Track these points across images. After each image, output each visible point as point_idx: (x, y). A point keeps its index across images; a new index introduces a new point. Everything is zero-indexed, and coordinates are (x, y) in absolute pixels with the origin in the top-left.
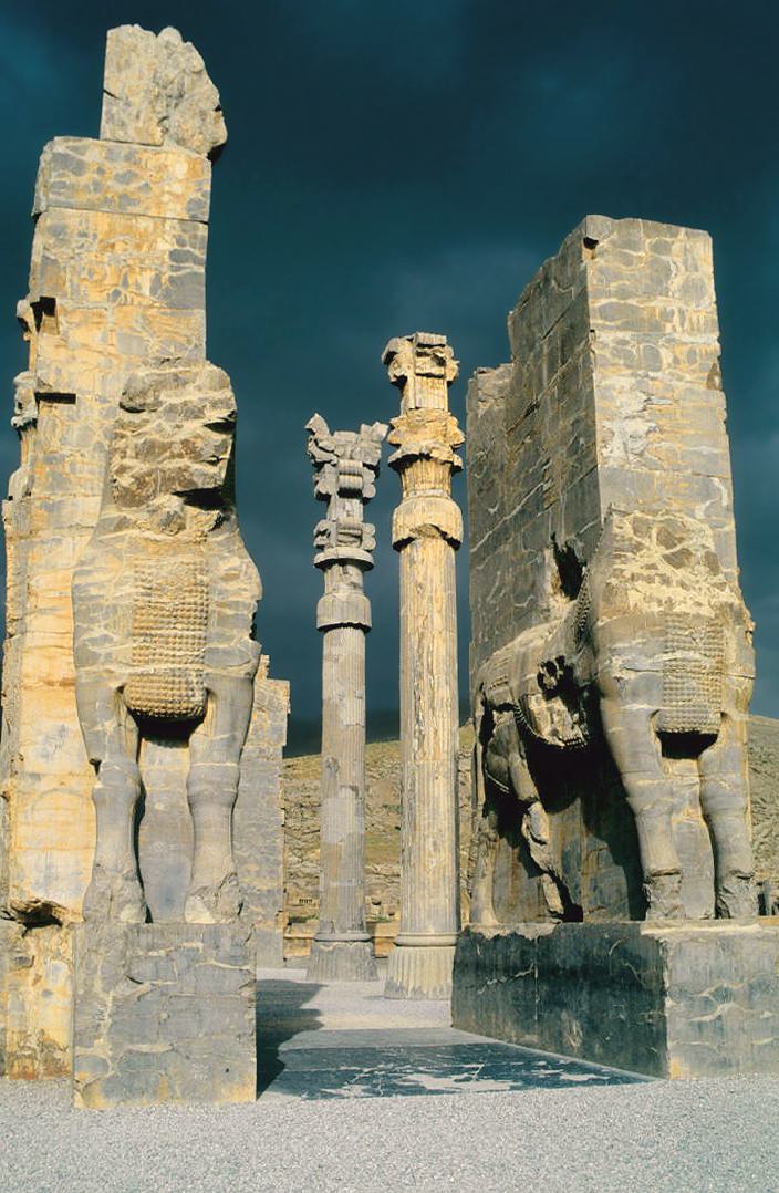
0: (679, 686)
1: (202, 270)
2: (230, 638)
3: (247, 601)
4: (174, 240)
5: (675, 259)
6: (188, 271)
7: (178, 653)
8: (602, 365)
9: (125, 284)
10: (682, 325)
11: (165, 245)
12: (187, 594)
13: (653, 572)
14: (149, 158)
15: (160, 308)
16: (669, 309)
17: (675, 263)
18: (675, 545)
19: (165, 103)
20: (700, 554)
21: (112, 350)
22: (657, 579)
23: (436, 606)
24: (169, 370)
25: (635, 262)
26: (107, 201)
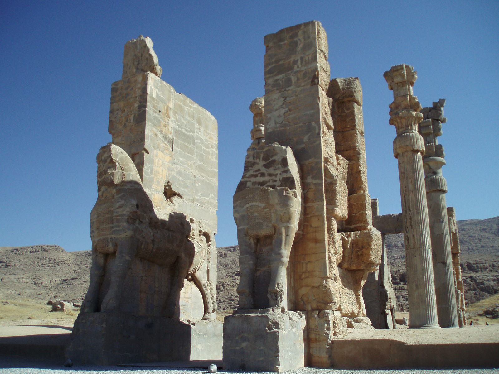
4: (139, 102)
6: (142, 110)
9: (127, 121)
10: (301, 64)
11: (136, 105)
13: (257, 173)
16: (296, 59)
17: (299, 39)
18: (269, 159)
20: (280, 160)
21: (123, 142)
22: (259, 175)
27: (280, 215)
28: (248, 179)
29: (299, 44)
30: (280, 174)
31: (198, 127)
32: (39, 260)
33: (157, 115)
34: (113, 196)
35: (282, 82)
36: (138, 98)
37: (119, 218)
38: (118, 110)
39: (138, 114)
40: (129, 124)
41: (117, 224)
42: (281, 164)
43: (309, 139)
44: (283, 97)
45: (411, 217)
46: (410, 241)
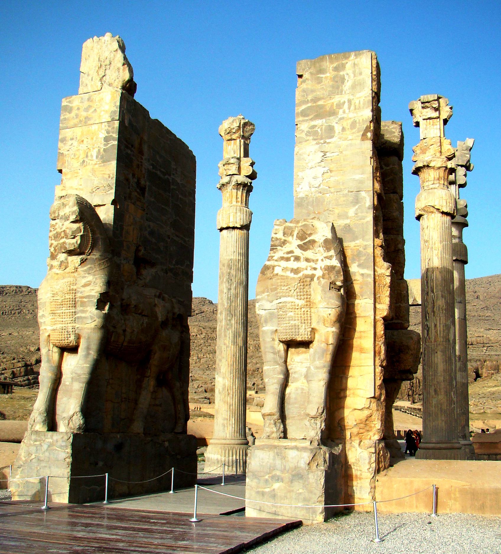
0: (284, 316)
1: (116, 143)
2: (87, 311)
5: (348, 72)
7: (64, 320)
8: (300, 142)
9: (87, 156)
10: (349, 108)
12: (66, 295)
13: (289, 255)
17: (348, 74)
19: (104, 69)
21: (81, 187)
23: (435, 252)
24: (62, 200)
25: (324, 80)
26: (81, 121)
27: (324, 317)
28: (276, 263)
29: (346, 81)
30: (322, 260)
31: (175, 167)
33: (129, 152)
35: (321, 130)
37: (85, 300)
38: (72, 139)
40: (91, 162)
42: (322, 247)
43: (356, 214)
44: (323, 152)
45: (433, 301)
46: (430, 332)
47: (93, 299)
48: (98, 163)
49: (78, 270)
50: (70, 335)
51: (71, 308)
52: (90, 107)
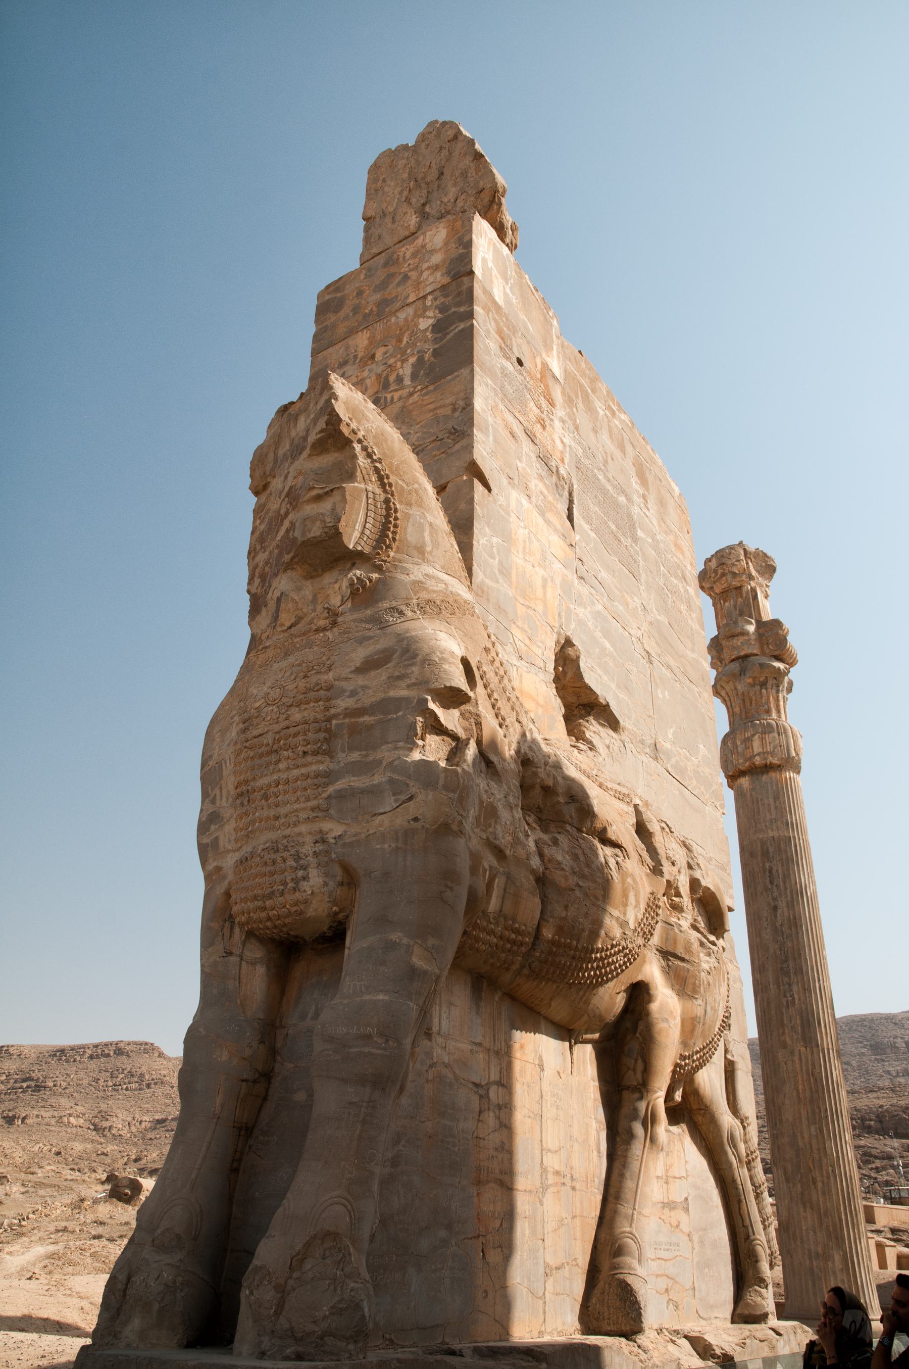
3: (404, 693)
11: (425, 324)
12: (294, 710)
14: (407, 250)
15: (422, 389)
32: (108, 1074)
34: (333, 616)
36: (435, 299)
39: (434, 350)
40: (396, 395)
41: (355, 756)
47: (400, 714)
48: (419, 387)
49: (340, 619)
50: (305, 868)
51: (309, 759)
52: (391, 276)
